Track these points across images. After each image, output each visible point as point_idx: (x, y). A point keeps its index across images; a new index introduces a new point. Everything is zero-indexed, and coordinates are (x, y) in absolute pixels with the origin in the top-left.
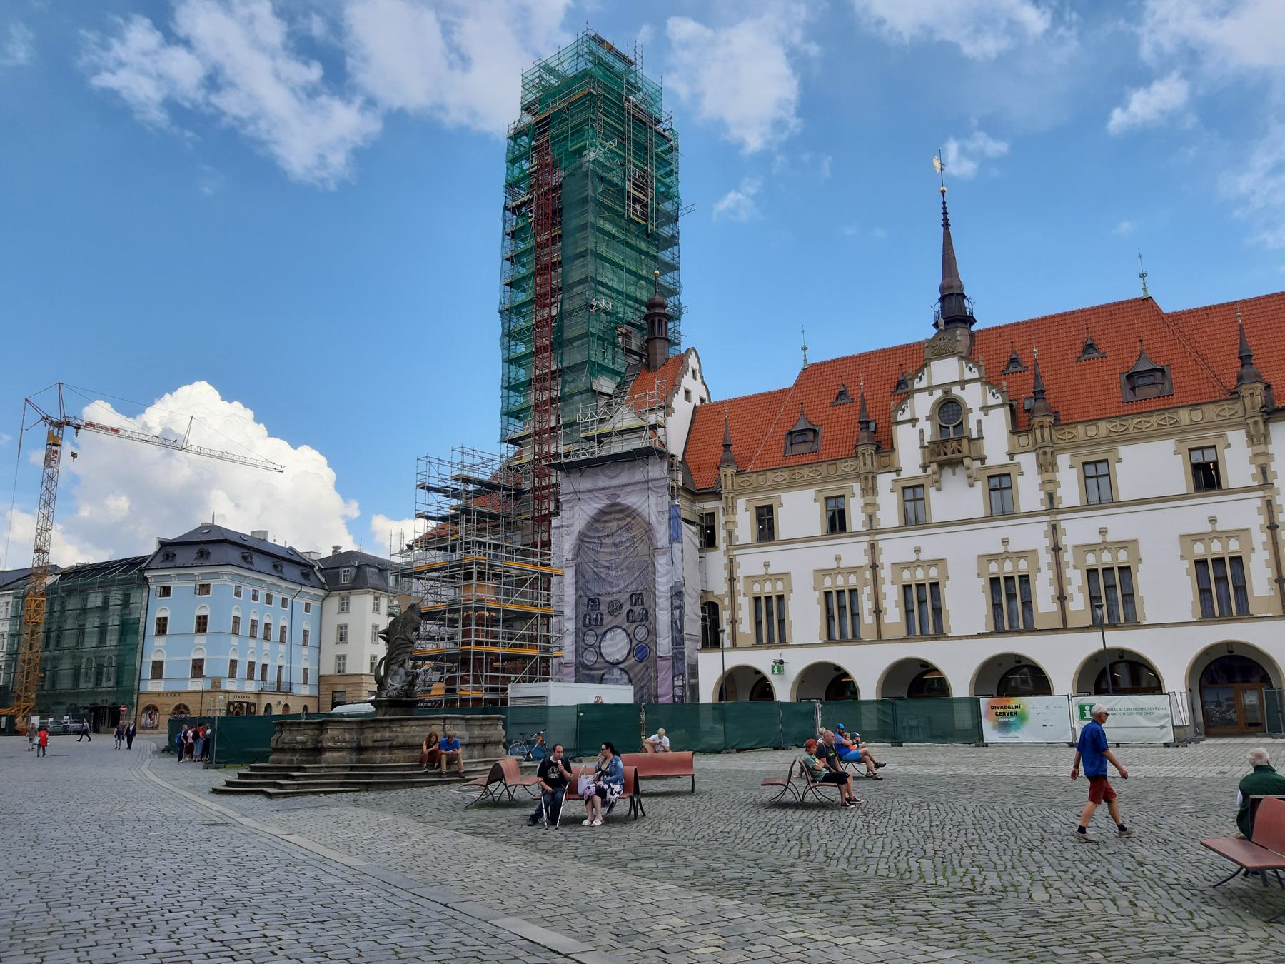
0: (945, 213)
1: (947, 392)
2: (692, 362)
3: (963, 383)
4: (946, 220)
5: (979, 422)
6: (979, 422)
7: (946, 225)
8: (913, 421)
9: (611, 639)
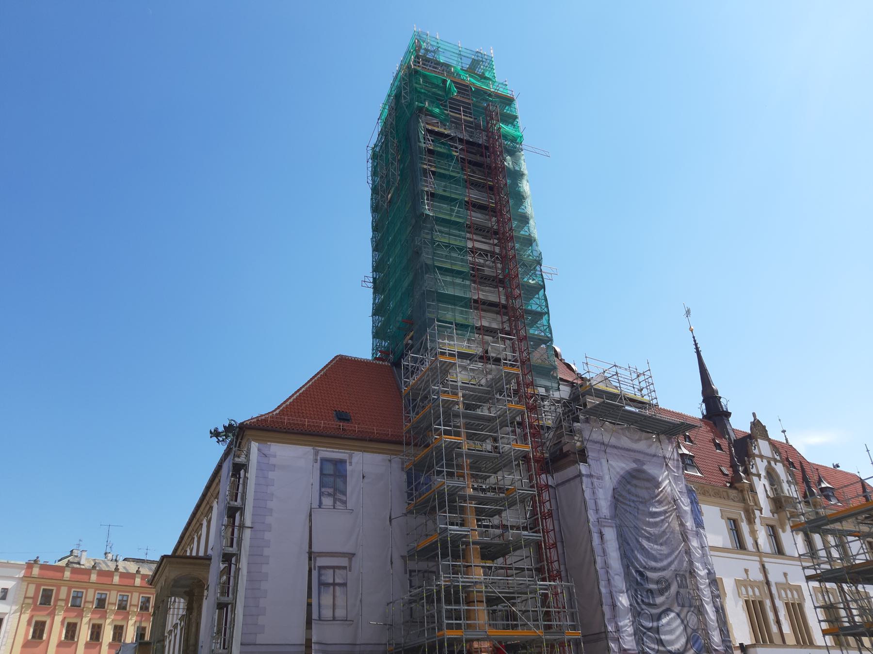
0: (696, 344)
4: (697, 348)
7: (698, 352)
9: (668, 624)
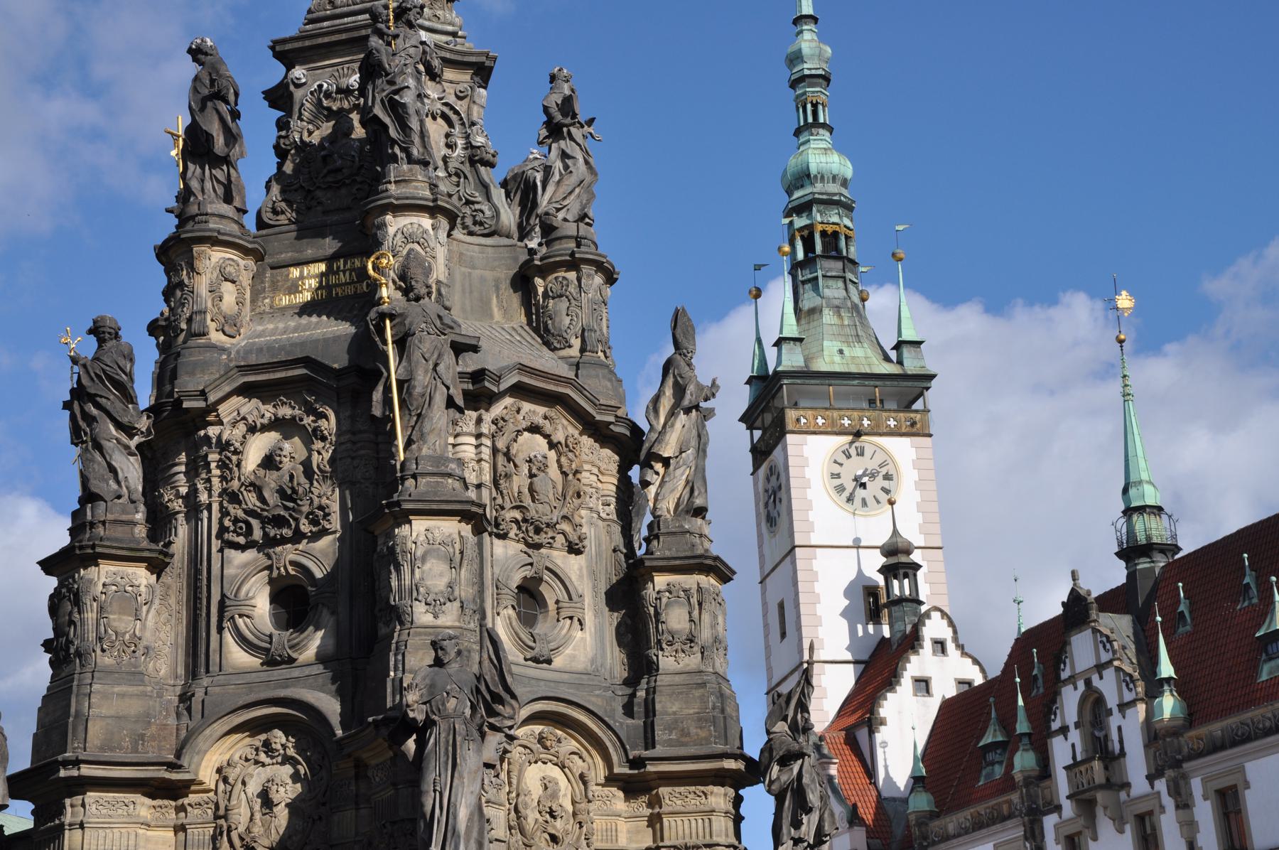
1: (1088, 683)
2: (934, 628)
3: (1100, 668)
5: (1120, 728)
6: (1120, 728)
8: (1064, 730)
